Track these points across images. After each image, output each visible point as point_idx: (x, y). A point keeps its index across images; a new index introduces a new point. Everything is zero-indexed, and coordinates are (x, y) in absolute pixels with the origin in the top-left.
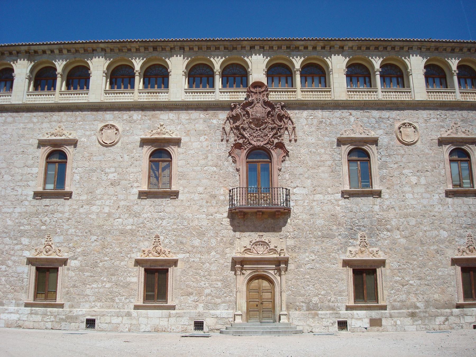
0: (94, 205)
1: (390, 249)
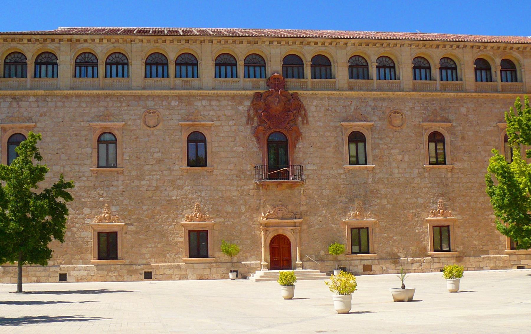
0: (144, 179)
1: (379, 213)
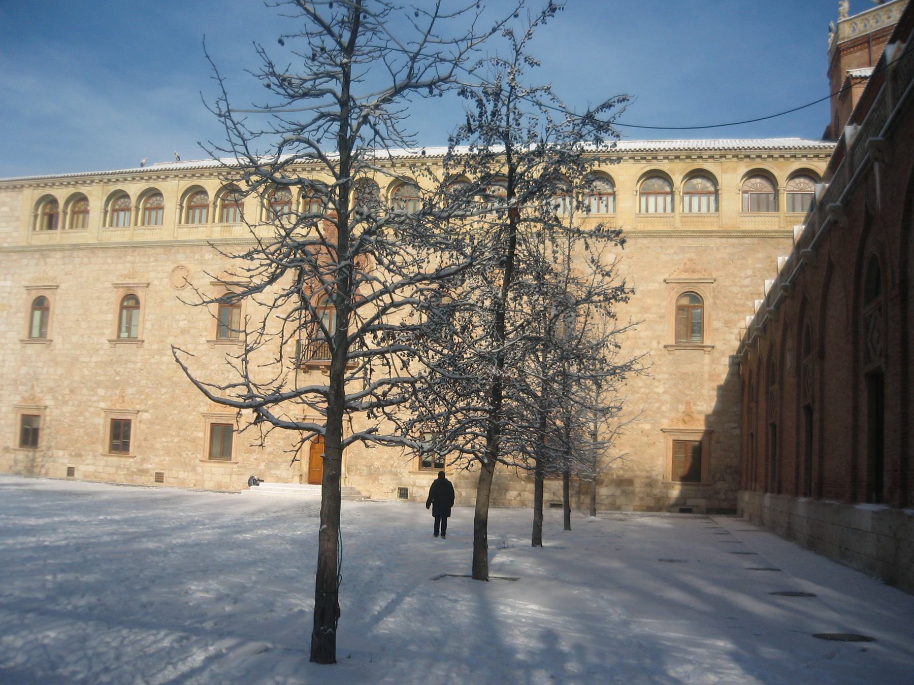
0: (165, 355)
